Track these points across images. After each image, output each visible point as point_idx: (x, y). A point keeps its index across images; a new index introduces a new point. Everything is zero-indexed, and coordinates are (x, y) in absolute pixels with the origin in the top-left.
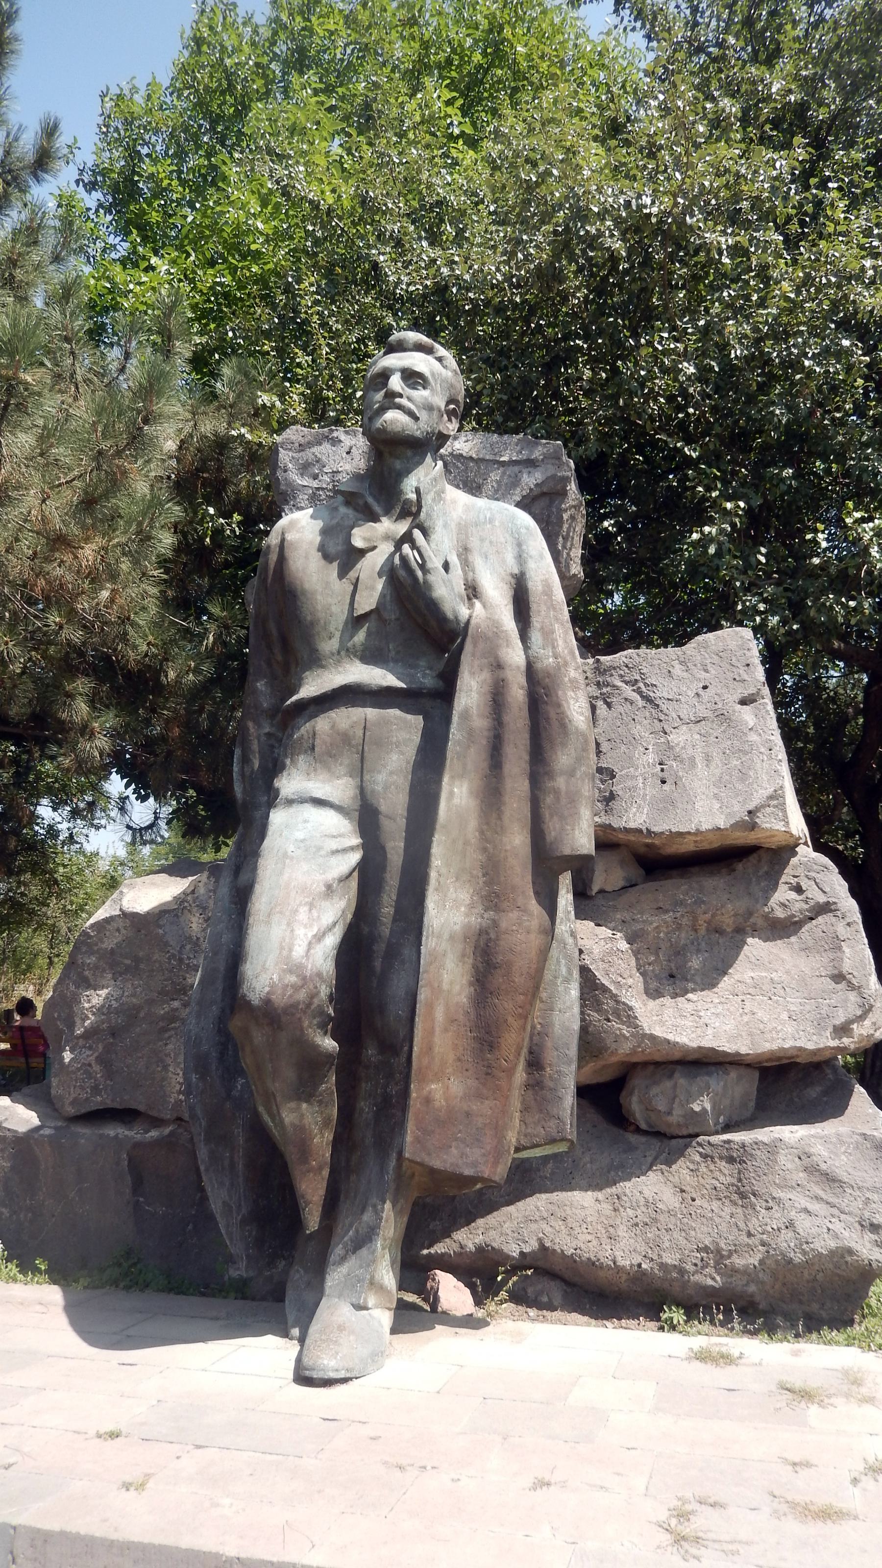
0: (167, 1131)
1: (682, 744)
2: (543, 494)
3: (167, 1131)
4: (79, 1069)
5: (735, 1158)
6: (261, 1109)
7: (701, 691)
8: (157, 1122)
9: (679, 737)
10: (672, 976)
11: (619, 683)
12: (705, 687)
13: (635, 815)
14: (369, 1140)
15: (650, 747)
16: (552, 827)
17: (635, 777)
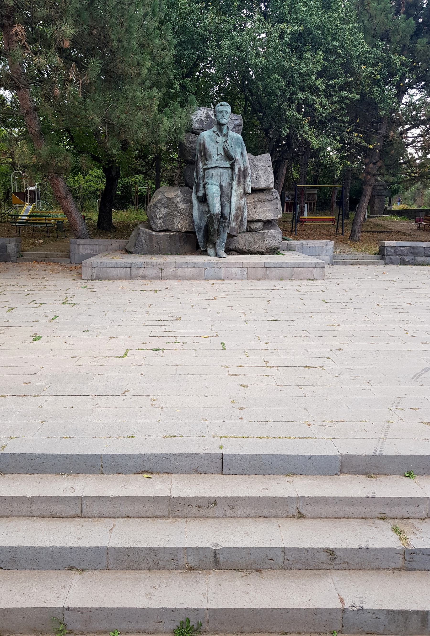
0: (174, 233)
3: (174, 233)
5: (263, 234)
6: (210, 227)
8: (174, 232)
9: (259, 172)
14: (222, 231)
16: (247, 189)
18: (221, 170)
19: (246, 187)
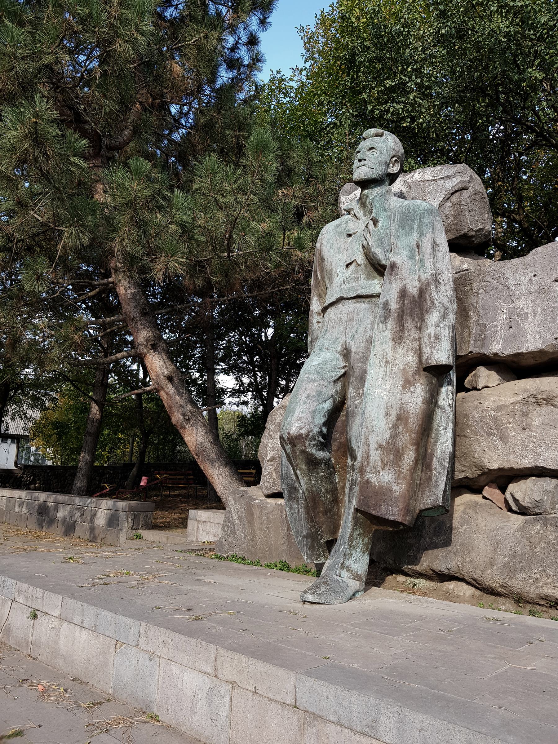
1: (521, 307)
2: (456, 191)
4: (267, 474)
7: (533, 278)
9: (521, 303)
10: (524, 429)
11: (489, 280)
12: (535, 276)
13: (495, 345)
15: (505, 311)
17: (496, 327)
18: (350, 306)
19: (424, 346)
